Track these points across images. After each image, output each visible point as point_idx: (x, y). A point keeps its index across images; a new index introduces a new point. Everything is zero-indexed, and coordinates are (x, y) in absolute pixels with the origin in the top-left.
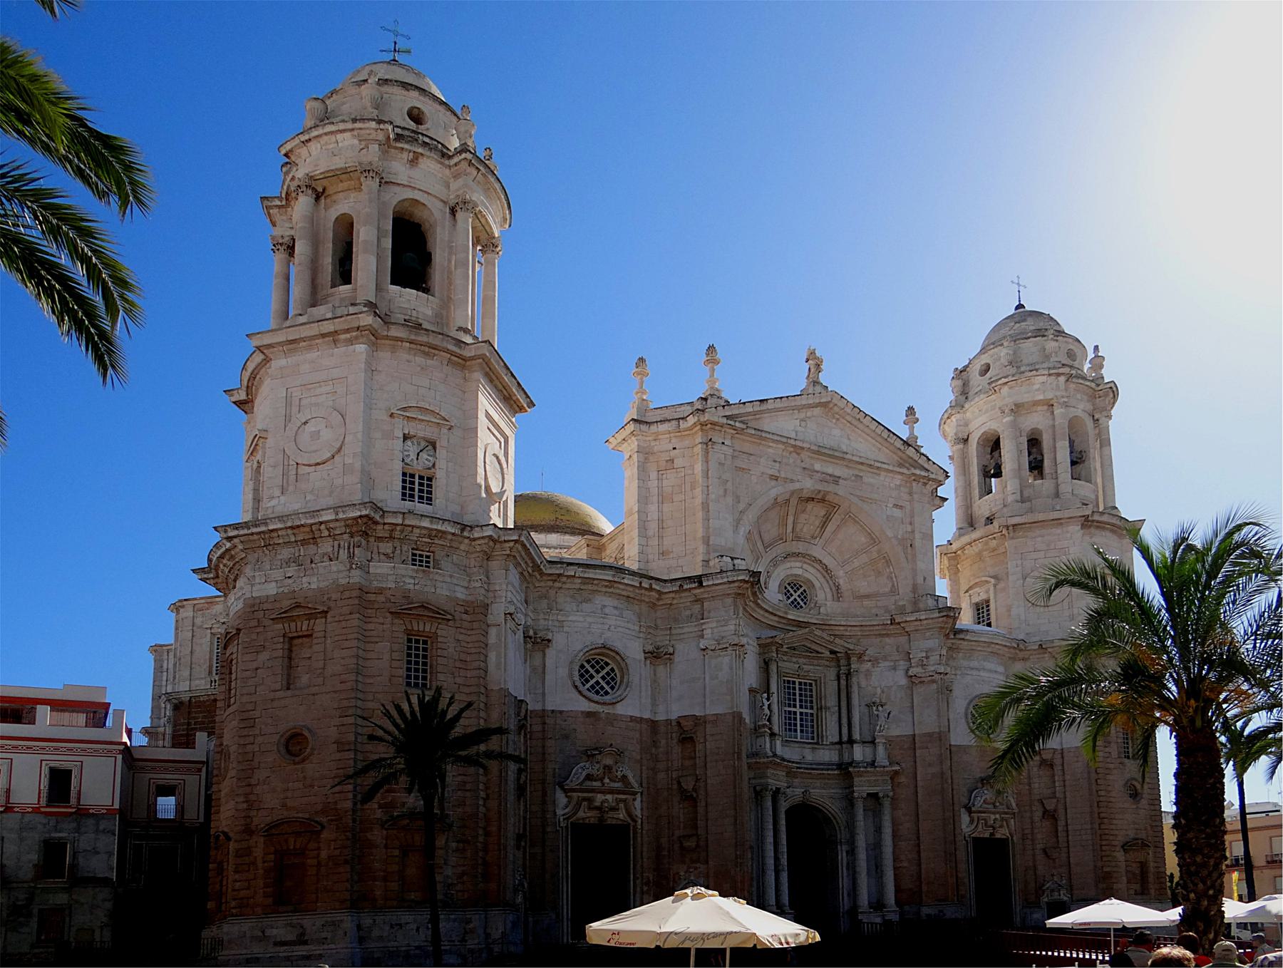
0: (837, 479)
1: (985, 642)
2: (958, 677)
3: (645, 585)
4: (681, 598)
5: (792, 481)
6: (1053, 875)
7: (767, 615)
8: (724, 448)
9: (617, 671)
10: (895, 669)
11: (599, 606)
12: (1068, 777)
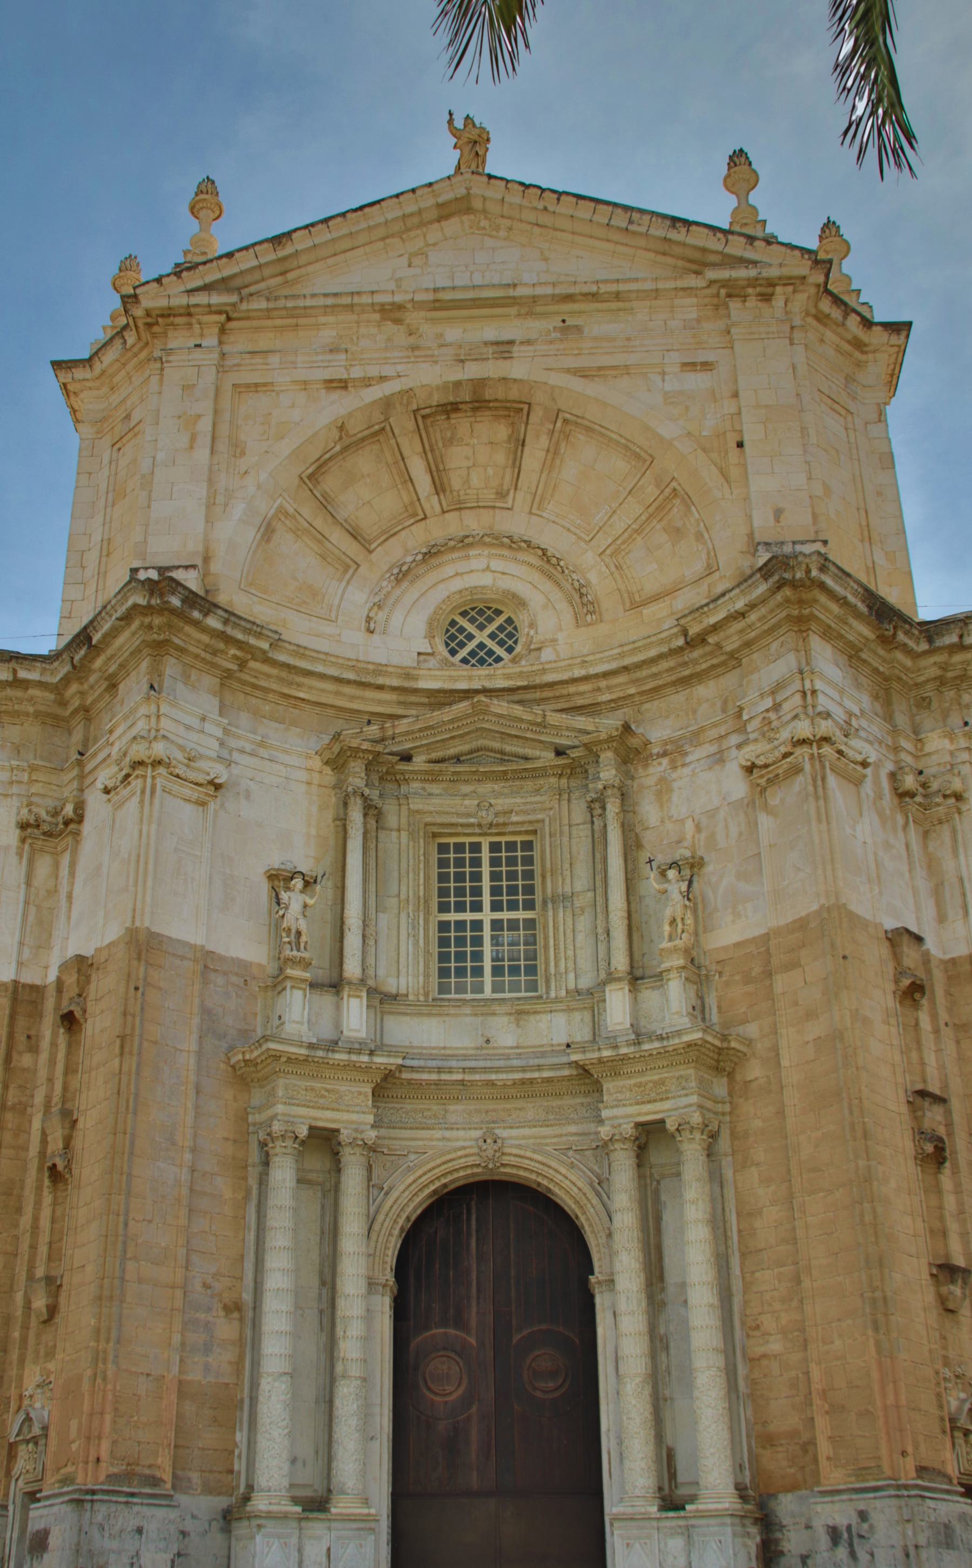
0: (505, 348)
4: (92, 687)
5: (383, 379)
7: (347, 690)
8: (197, 354)
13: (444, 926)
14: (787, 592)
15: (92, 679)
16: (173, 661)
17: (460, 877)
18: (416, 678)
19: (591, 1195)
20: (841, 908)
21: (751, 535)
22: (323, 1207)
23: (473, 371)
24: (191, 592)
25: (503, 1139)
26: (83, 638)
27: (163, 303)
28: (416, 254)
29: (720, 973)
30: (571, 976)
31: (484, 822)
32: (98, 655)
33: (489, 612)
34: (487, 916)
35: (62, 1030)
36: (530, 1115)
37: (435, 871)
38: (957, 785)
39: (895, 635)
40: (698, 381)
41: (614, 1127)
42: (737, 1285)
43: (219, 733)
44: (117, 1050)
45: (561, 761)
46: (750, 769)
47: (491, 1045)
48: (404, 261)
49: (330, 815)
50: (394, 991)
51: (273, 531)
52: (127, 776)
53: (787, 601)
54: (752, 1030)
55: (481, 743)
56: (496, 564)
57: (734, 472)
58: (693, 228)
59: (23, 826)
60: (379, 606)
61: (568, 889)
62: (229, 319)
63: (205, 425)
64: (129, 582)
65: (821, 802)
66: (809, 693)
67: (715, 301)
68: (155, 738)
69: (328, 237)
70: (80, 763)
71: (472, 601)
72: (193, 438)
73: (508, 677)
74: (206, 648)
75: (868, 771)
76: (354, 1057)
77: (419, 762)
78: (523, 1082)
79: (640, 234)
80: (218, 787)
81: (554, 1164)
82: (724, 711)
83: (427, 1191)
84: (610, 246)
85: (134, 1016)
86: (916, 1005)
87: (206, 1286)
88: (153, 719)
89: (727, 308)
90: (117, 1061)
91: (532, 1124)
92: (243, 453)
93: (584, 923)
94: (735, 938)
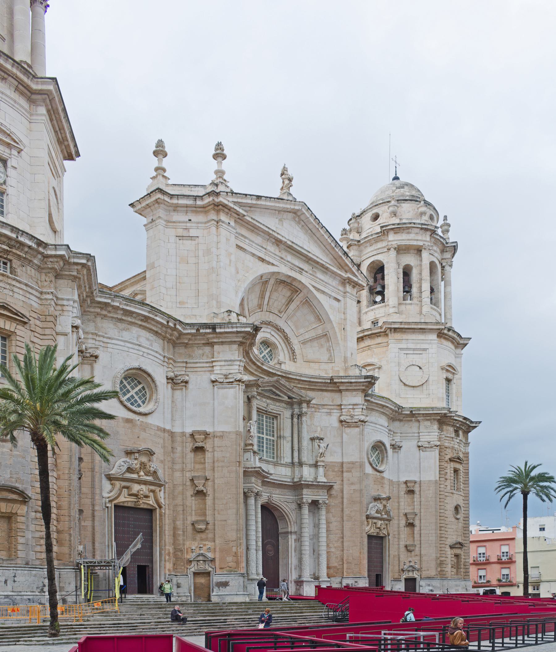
6: (410, 562)
9: (147, 390)
10: (330, 415)
11: (136, 336)
12: (423, 499)
45: (289, 400)
55: (271, 388)
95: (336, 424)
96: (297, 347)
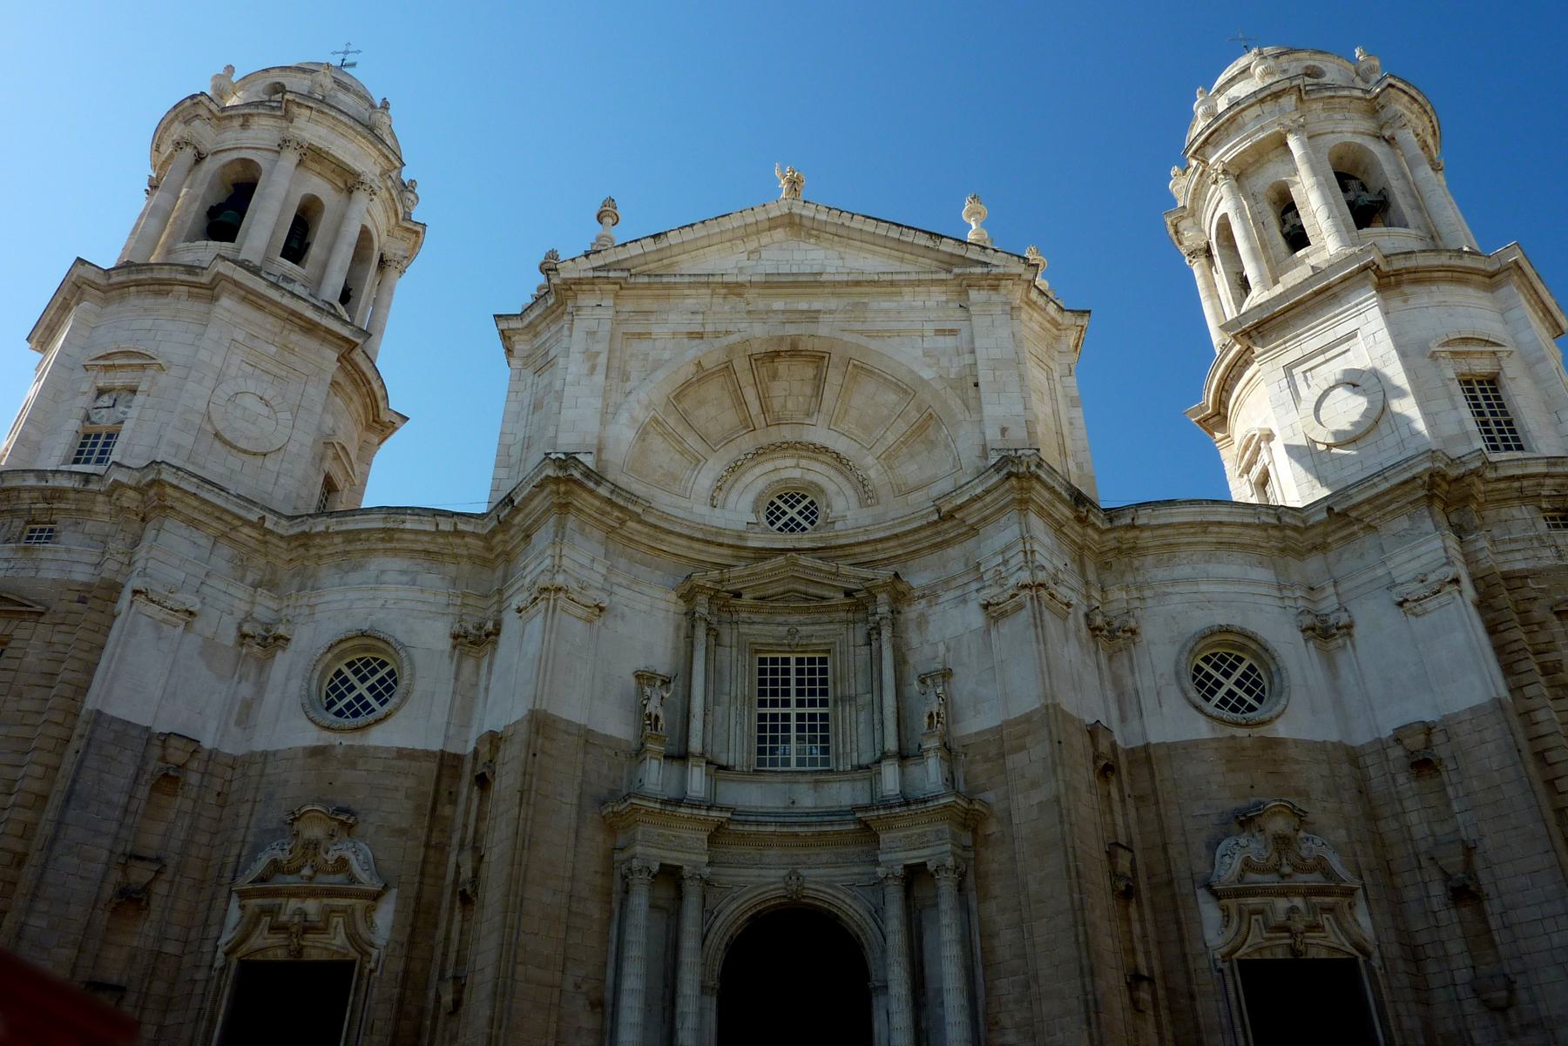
1: (1191, 524)
2: (1150, 602)
3: (446, 526)
4: (512, 538)
7: (697, 545)
13: (762, 717)
14: (1014, 481)
15: (512, 532)
16: (573, 518)
17: (774, 682)
18: (745, 539)
19: (869, 920)
20: (1056, 706)
21: (984, 446)
22: (668, 926)
23: (791, 330)
24: (588, 468)
25: (804, 877)
26: (509, 500)
27: (575, 275)
28: (752, 252)
29: (966, 754)
30: (855, 755)
31: (793, 643)
32: (517, 514)
33: (798, 497)
34: (793, 711)
35: (476, 788)
36: (825, 858)
37: (756, 677)
38: (1133, 624)
39: (1087, 517)
40: (948, 342)
41: (887, 868)
42: (981, 991)
43: (604, 571)
44: (518, 801)
46: (986, 607)
47: (796, 805)
48: (745, 256)
49: (682, 635)
50: (725, 764)
51: (648, 433)
52: (536, 598)
53: (1013, 488)
54: (990, 796)
56: (803, 463)
57: (972, 403)
58: (944, 240)
59: (455, 637)
60: (720, 488)
61: (853, 692)
62: (621, 288)
63: (603, 359)
64: (545, 459)
65: (1039, 629)
66: (1029, 553)
67: (959, 289)
68: (558, 571)
69: (692, 236)
70: (500, 591)
71: (786, 488)
72: (593, 369)
73: (812, 540)
74: (598, 510)
75: (1071, 610)
76: (695, 812)
77: (747, 598)
78: (820, 834)
79: (908, 243)
80: (601, 609)
81: (841, 896)
82: (966, 565)
83: (746, 916)
84: (887, 251)
85: (531, 775)
86: (1107, 780)
87: (577, 986)
88: (557, 558)
89: (967, 294)
90: (517, 809)
91: (827, 865)
92: (628, 380)
93: (863, 716)
94: (975, 730)
95: (977, 619)
96: (874, 472)
